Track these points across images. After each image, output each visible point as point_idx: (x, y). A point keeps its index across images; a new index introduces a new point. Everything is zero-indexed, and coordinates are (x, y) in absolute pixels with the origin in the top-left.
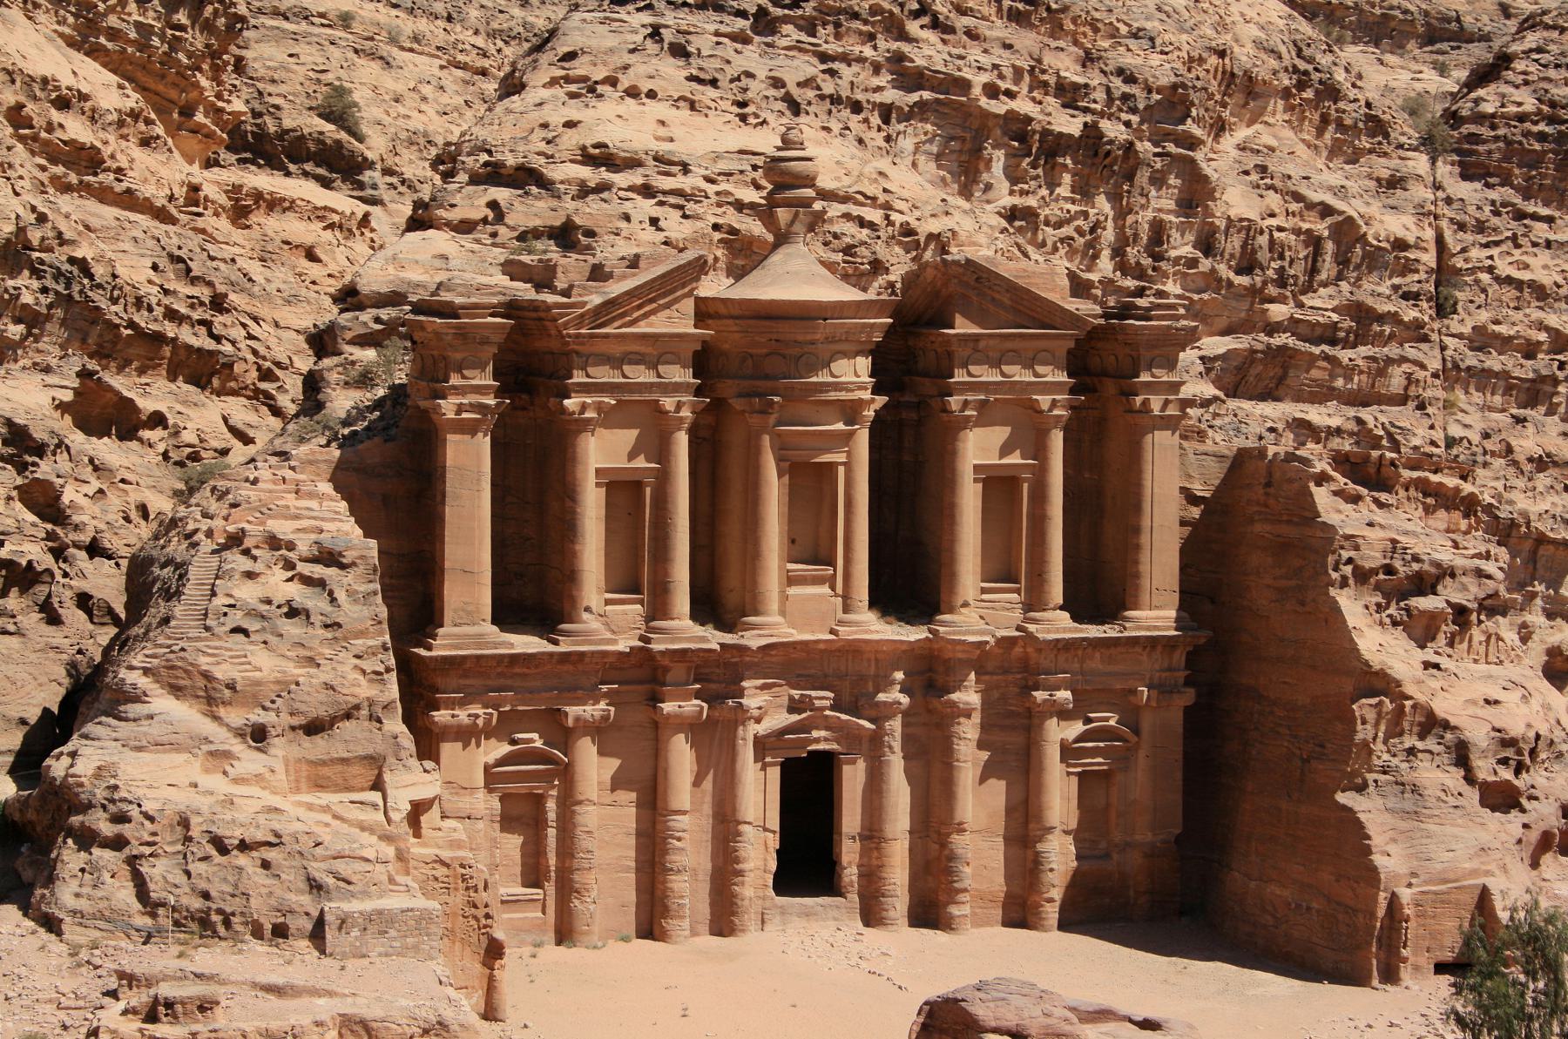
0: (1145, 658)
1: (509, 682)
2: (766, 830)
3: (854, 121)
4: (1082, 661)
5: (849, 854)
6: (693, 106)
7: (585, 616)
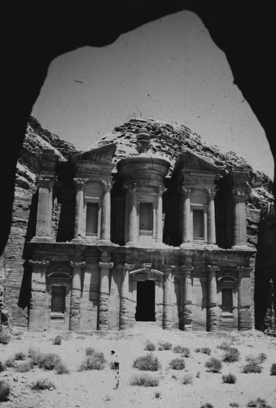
0: (239, 258)
1: (54, 253)
2: (133, 301)
3: (169, 156)
4: (221, 258)
5: (158, 309)
6: (130, 146)
7: (79, 237)
